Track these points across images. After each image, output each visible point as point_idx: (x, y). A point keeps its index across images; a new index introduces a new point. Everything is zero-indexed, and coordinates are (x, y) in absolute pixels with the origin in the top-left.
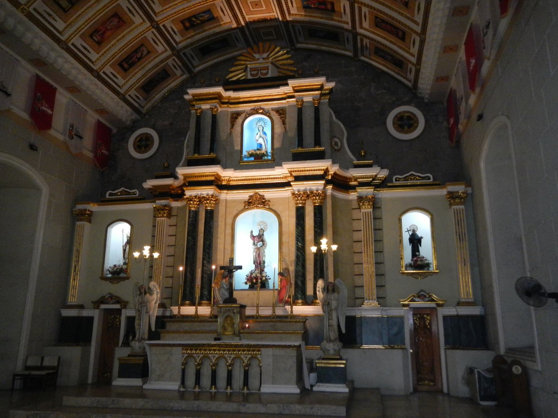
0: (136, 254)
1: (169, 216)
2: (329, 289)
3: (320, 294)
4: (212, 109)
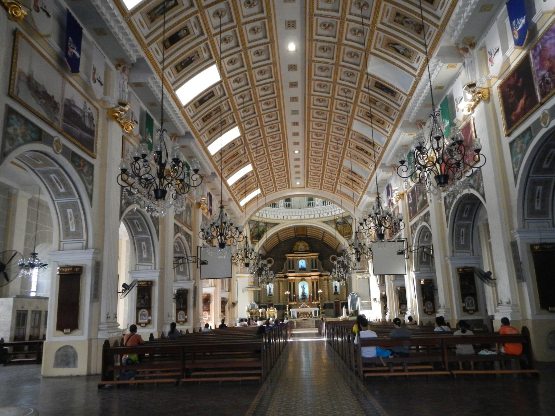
2: (321, 299)
3: (319, 299)
4: (292, 259)
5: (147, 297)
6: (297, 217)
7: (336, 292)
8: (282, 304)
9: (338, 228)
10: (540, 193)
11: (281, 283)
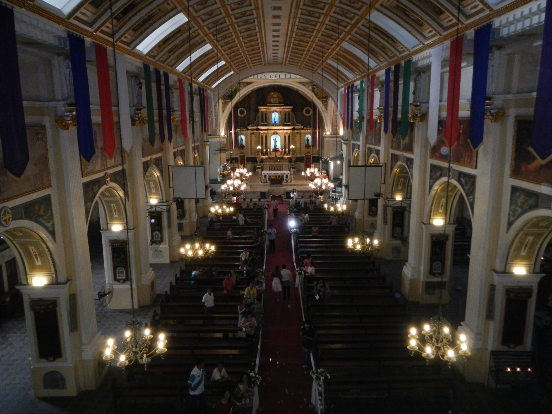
2: (292, 154)
5: (123, 256)
6: (272, 76)
7: (308, 146)
8: (254, 156)
9: (315, 90)
10: (529, 244)
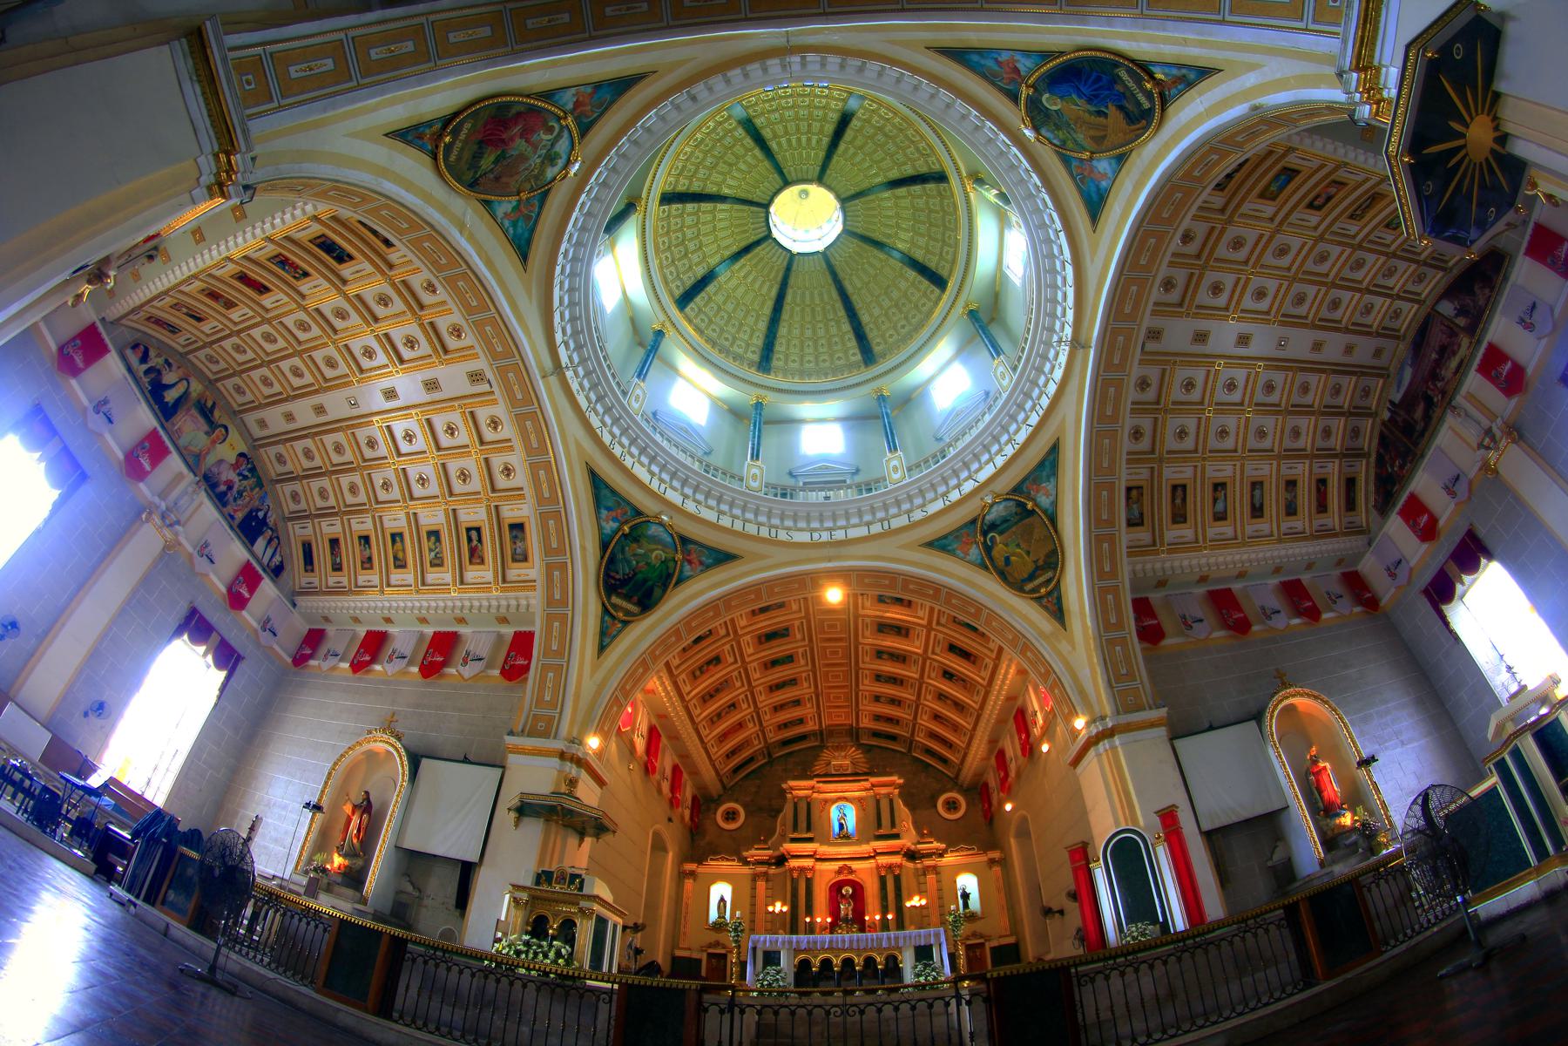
0: (770, 909)
1: (767, 881)
4: (807, 797)
9: (995, 553)
11: (761, 884)
